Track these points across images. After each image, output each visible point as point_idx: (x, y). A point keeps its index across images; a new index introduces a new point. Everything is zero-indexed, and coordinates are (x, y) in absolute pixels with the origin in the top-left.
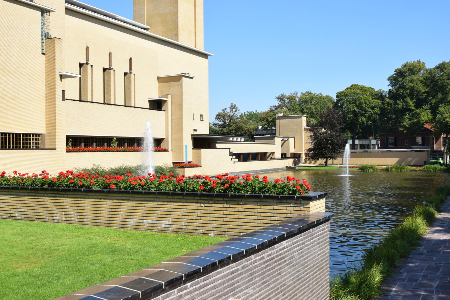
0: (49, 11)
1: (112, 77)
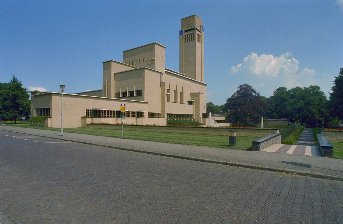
0: (162, 73)
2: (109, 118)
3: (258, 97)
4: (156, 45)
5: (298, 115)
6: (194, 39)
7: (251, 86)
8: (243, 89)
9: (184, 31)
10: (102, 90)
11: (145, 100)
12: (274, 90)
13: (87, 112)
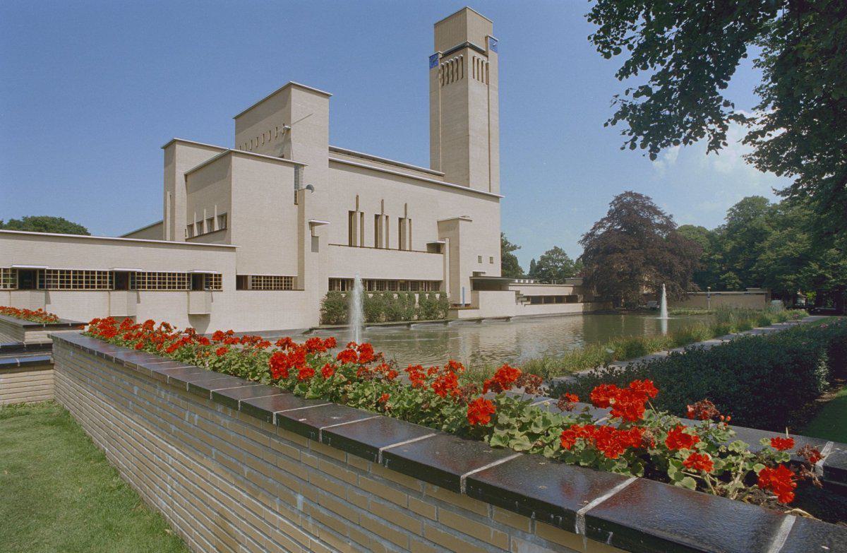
1: (384, 222)
2: (69, 293)
3: (668, 225)
4: (294, 91)
5: (793, 277)
6: (464, 76)
7: (648, 198)
8: (623, 206)
9: (440, 56)
10: (160, 224)
11: (232, 242)
12: (731, 207)
13: (220, 284)
